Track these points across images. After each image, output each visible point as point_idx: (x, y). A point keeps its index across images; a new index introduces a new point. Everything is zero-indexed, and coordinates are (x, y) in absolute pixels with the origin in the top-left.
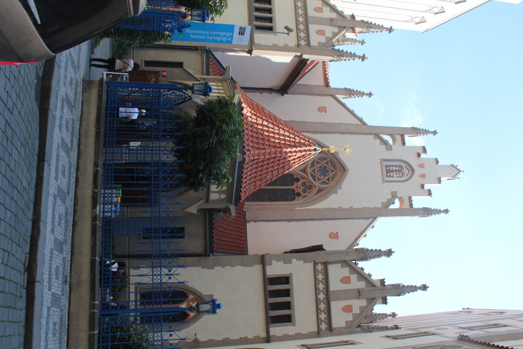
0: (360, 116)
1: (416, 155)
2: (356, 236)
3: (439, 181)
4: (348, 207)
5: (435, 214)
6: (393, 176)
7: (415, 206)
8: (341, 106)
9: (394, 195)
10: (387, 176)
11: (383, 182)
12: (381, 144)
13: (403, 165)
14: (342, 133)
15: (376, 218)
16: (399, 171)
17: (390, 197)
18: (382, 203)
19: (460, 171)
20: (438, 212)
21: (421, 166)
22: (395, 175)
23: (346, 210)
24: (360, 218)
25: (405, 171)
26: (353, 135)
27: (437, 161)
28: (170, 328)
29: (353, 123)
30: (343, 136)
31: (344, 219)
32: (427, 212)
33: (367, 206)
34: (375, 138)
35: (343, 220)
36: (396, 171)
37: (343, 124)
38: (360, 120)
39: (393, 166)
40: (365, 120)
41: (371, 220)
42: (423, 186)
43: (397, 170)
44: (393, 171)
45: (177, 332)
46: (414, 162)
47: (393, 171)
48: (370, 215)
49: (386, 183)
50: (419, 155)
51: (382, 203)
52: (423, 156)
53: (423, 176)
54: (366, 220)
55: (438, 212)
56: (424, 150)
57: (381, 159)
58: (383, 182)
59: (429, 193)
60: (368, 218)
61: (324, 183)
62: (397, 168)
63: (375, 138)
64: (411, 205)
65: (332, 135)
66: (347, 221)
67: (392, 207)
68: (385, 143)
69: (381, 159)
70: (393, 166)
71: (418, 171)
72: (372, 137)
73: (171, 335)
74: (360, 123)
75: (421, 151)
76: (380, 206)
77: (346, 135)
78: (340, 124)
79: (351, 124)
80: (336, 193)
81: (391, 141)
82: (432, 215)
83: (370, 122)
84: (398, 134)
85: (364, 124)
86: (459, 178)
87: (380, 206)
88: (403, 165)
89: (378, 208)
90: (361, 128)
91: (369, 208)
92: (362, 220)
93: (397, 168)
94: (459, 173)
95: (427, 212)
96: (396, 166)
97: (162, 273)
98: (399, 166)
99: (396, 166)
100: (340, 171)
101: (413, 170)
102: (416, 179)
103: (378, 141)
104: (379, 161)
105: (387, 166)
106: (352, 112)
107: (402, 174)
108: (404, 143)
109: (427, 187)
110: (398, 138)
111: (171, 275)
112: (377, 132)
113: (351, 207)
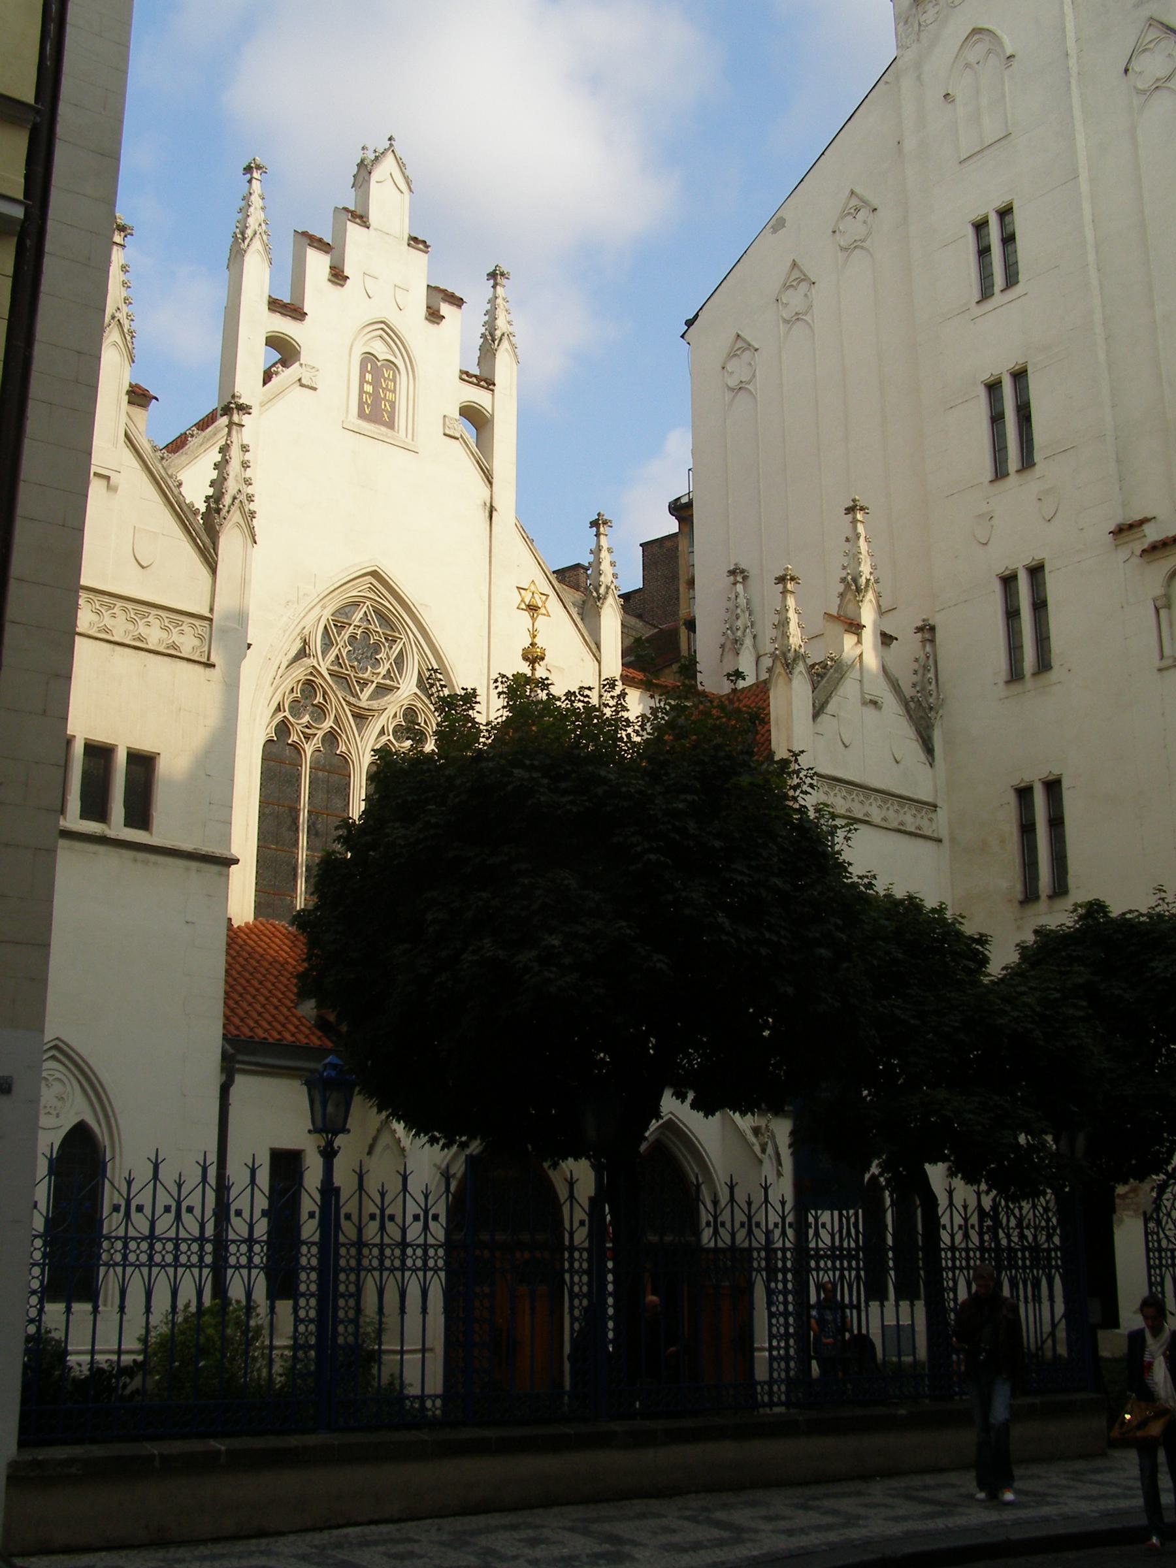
3: (414, 241)
6: (393, 404)
10: (391, 425)
16: (377, 373)
22: (390, 396)
25: (381, 351)
28: (116, 1208)
36: (375, 384)
39: (362, 391)
44: (375, 395)
45: (233, 1193)
61: (400, 661)
62: (369, 377)
73: (239, 1213)
93: (369, 377)
97: (121, 1233)
99: (362, 380)
105: (361, 415)
111: (128, 1202)
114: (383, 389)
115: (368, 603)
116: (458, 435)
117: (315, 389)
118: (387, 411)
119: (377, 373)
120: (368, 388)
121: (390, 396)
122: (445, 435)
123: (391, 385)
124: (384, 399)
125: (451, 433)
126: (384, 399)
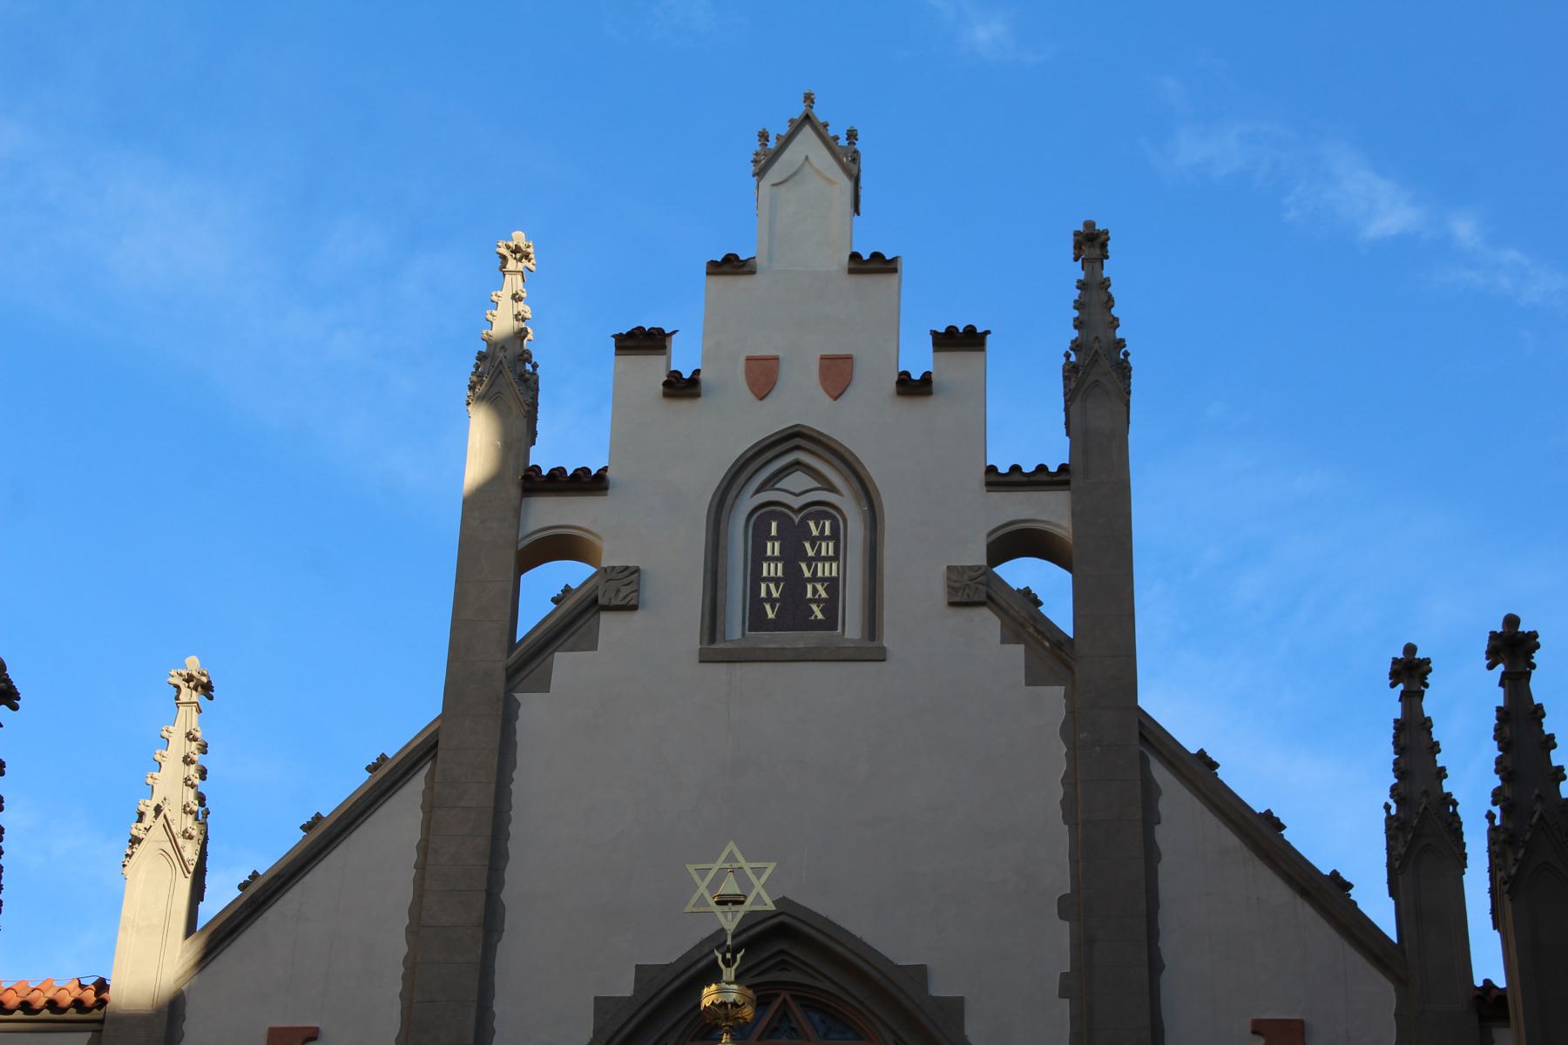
0: (355, 779)
1: (683, 406)
2: (1279, 892)
3: (880, 265)
4: (1062, 932)
5: (1114, 323)
7: (1055, 451)
8: (272, 915)
9: (973, 590)
10: (830, 622)
11: (880, 656)
12: (593, 646)
13: (748, 502)
14: (491, 921)
15: (1153, 738)
16: (794, 538)
17: (986, 622)
18: (1032, 679)
19: (807, 118)
20: (1094, 301)
21: (763, 375)
22: (824, 570)
23: (1083, 946)
24: (1151, 854)
25: (796, 489)
26: (512, 846)
27: (730, 266)
29: (417, 836)
30: (513, 919)
31: (1155, 966)
32: (1097, 375)
33: (1059, 793)
34: (545, 687)
35: (1165, 978)
36: (792, 556)
37: (416, 909)
38: (387, 780)
39: (756, 578)
40: (395, 740)
41: (1159, 772)
42: (913, 387)
43: (788, 552)
44: (793, 582)
46: (732, 425)
47: (793, 582)
48: (1128, 774)
49: (889, 639)
50: (681, 387)
51: (1032, 679)
52: (684, 357)
53: (837, 373)
54: (1163, 806)
55: (1094, 301)
56: (643, 341)
57: (705, 658)
58: (880, 656)
59: (961, 340)
60: (1150, 792)
62: (774, 548)
63: (543, 686)
64: (1041, 479)
65: (500, 1005)
66: (1168, 945)
67: (1060, 610)
68: (575, 619)
69: (705, 658)
70: (756, 578)
71: (799, 402)
72: (531, 705)
74: (418, 783)
75: (651, 370)
76: (1055, 695)
77: (506, 895)
78: (416, 930)
79: (424, 848)
80: (954, 1008)
81: (573, 573)
82: (1121, 343)
83: (408, 701)
84: (518, 513)
85: (425, 751)
86: (852, 135)
87: (1055, 695)
88: (748, 502)
89: (1072, 713)
90: (457, 776)
91: (1069, 781)
92: (1161, 834)
94: (820, 130)
95: (1097, 375)
96: (758, 556)
98: (759, 536)
99: (758, 556)
100: (783, 966)
101: (796, 437)
102: (862, 421)
103: (564, 663)
104: (719, 672)
105: (756, 620)
106: (325, 837)
107: (818, 518)
108: (588, 483)
109: (918, 359)
110: (548, 514)
112: (499, 662)
113: (1066, 908)
114: (809, 561)
115: (784, 995)
116: (983, 597)
117: (634, 608)
118: (818, 601)
119: (794, 538)
120: (772, 569)
121: (824, 570)
122: (952, 604)
123: (827, 549)
124: (814, 579)
125: (965, 599)
126: (814, 579)
